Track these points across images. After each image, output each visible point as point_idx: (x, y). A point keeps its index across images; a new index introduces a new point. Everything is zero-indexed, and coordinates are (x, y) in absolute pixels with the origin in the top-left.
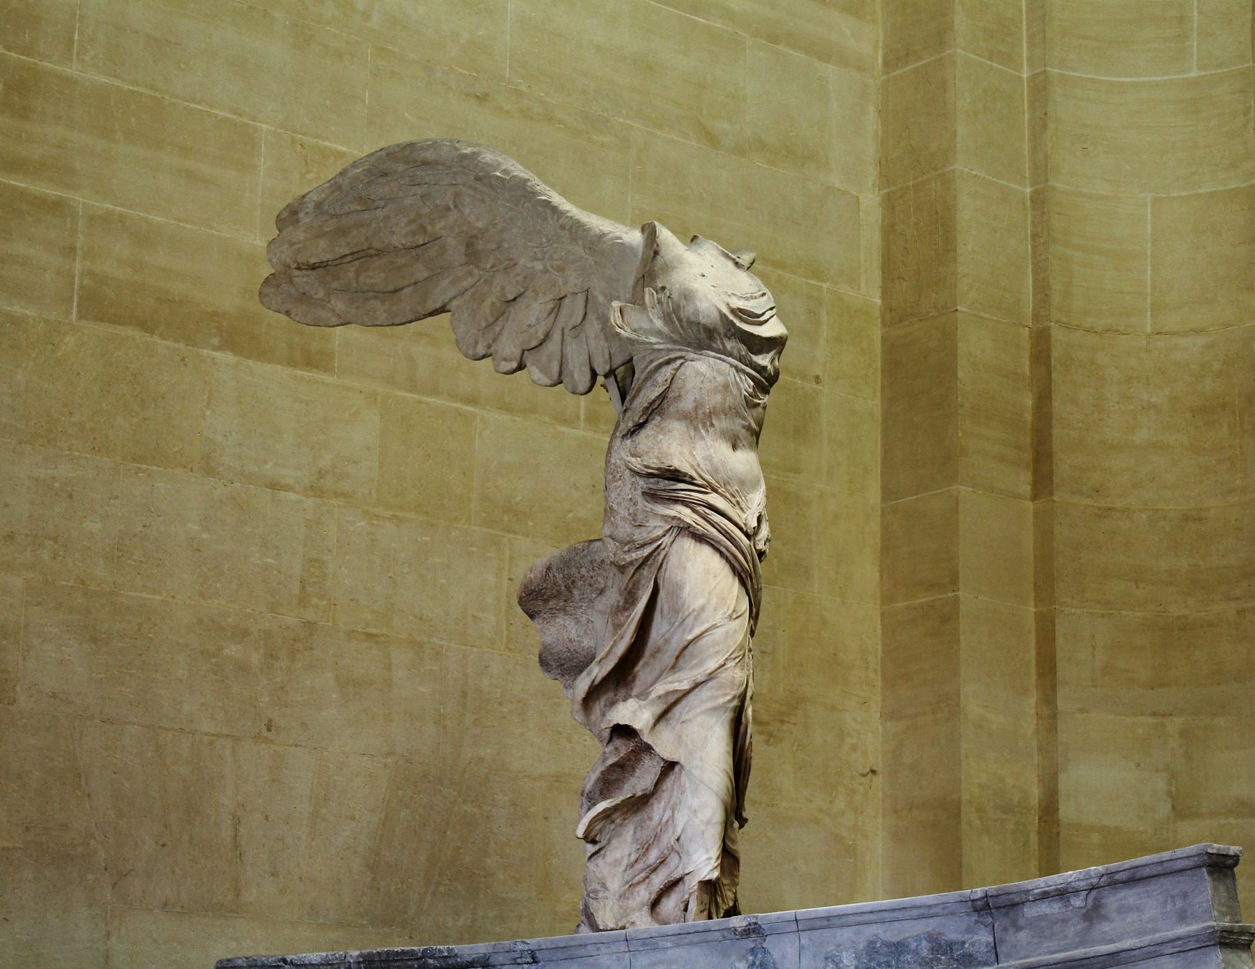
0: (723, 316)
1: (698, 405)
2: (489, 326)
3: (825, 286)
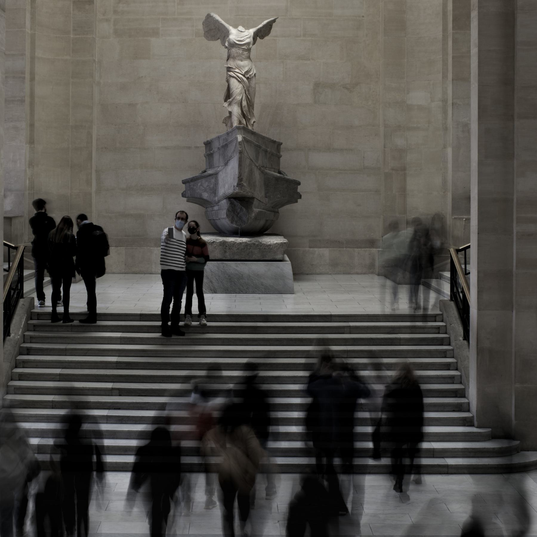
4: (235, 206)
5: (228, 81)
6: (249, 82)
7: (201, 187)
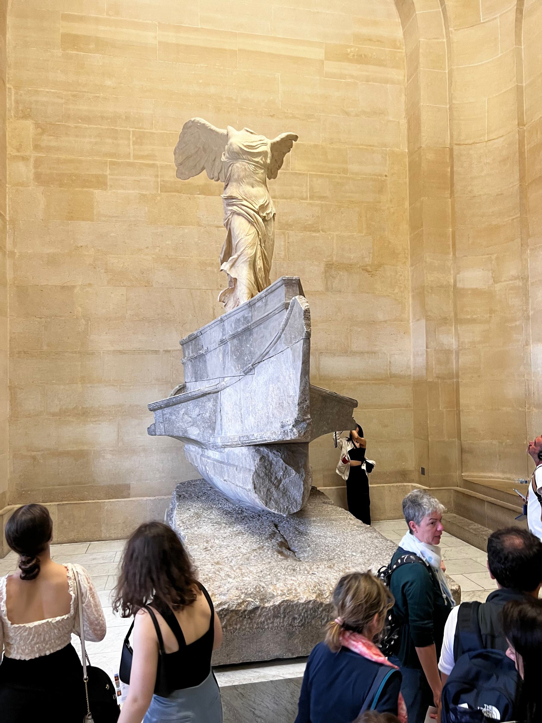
0: (241, 148)
1: (239, 176)
2: (212, 169)
4: (271, 464)
5: (228, 224)
7: (186, 417)
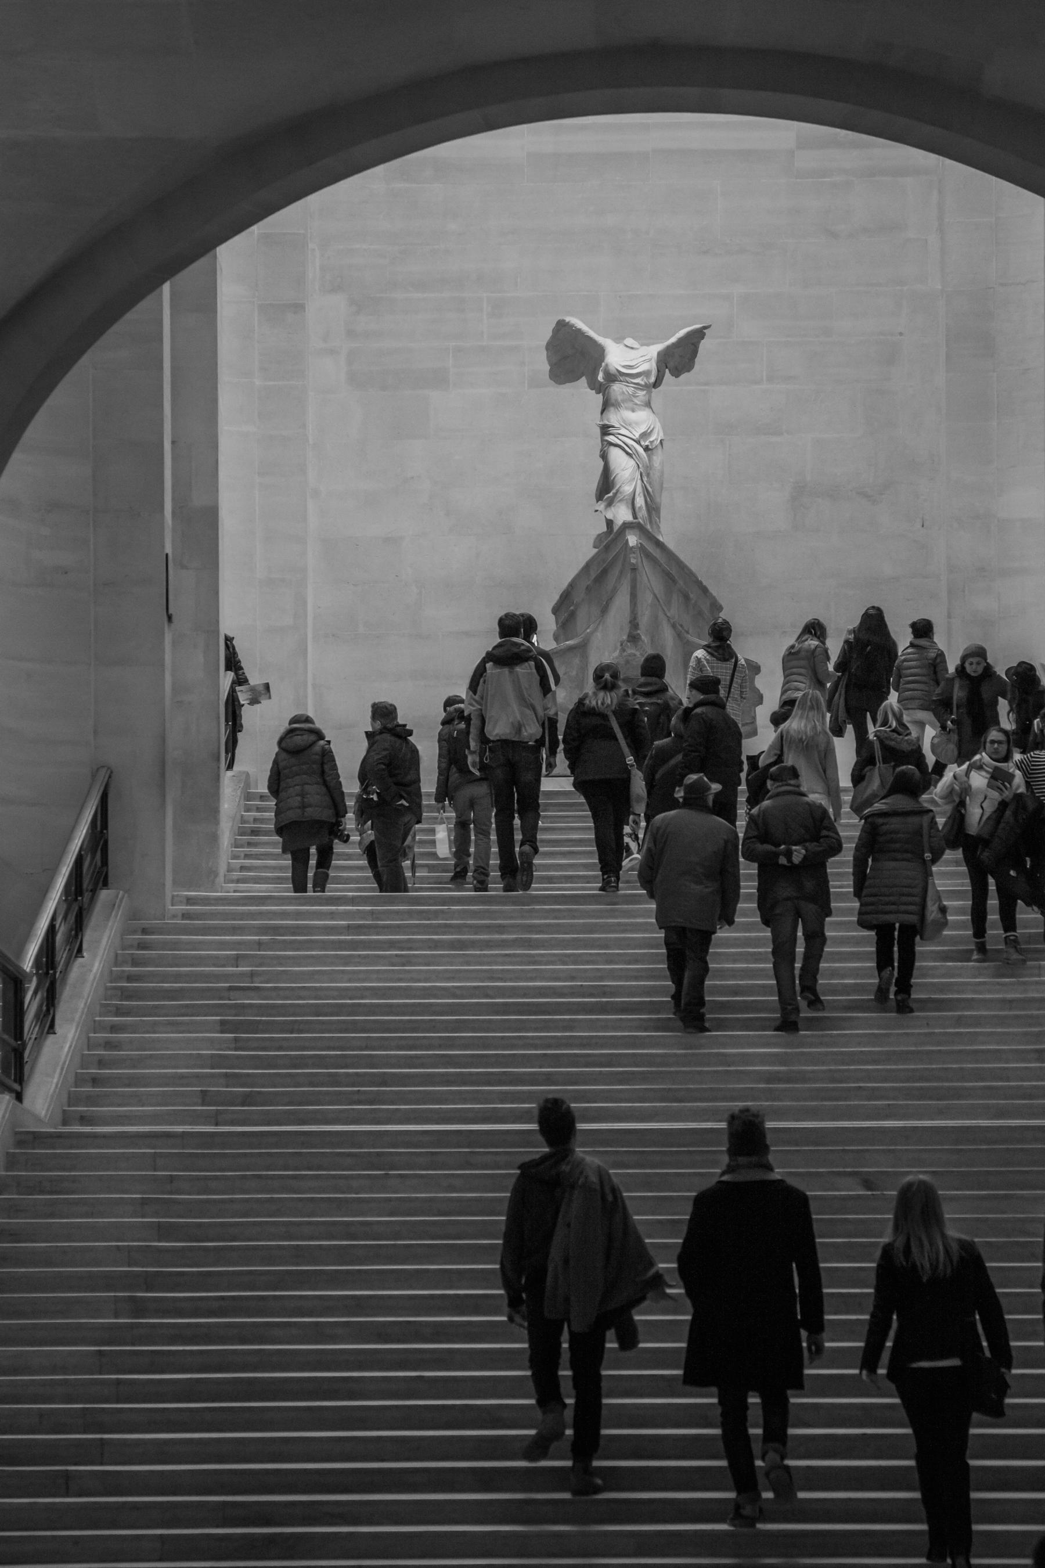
3: (905, 288)
5: (604, 456)
6: (649, 456)
